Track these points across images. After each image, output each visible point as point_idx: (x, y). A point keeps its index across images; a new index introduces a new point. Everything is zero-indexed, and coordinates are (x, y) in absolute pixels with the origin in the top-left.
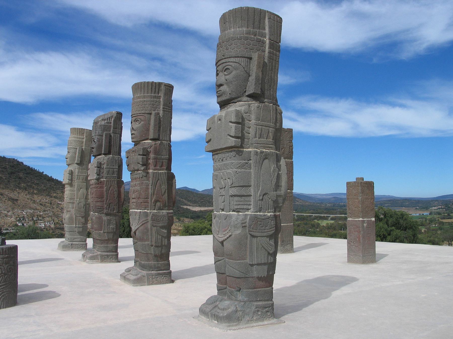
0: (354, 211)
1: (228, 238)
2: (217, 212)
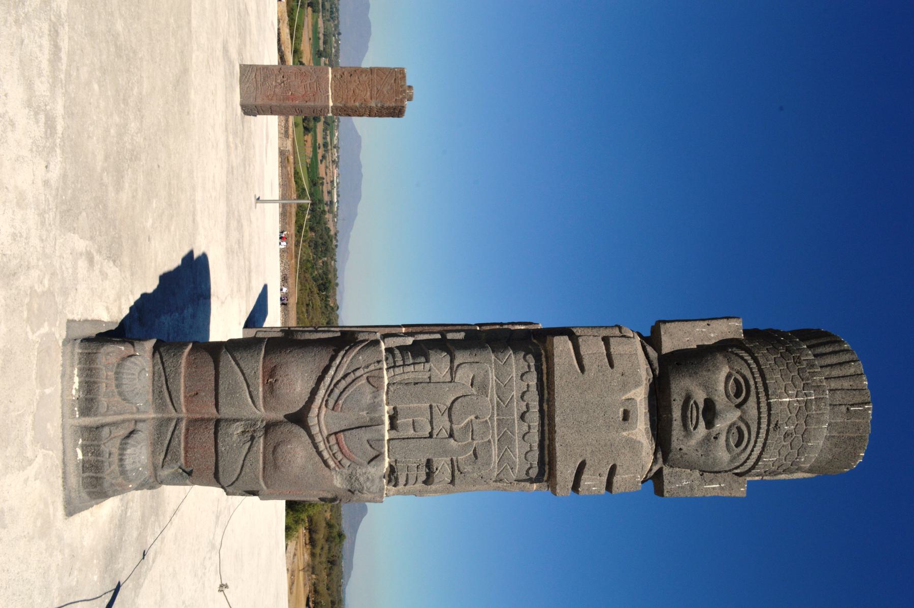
0: (347, 87)
1: (320, 454)
2: (387, 393)
